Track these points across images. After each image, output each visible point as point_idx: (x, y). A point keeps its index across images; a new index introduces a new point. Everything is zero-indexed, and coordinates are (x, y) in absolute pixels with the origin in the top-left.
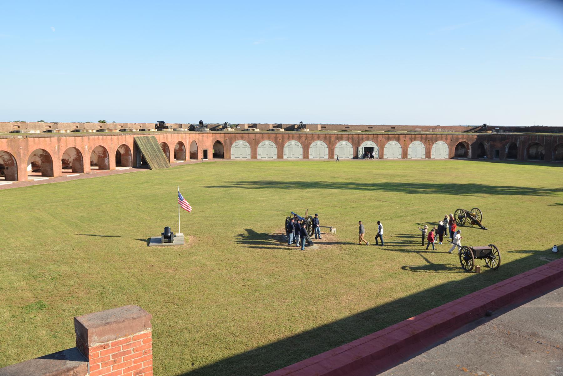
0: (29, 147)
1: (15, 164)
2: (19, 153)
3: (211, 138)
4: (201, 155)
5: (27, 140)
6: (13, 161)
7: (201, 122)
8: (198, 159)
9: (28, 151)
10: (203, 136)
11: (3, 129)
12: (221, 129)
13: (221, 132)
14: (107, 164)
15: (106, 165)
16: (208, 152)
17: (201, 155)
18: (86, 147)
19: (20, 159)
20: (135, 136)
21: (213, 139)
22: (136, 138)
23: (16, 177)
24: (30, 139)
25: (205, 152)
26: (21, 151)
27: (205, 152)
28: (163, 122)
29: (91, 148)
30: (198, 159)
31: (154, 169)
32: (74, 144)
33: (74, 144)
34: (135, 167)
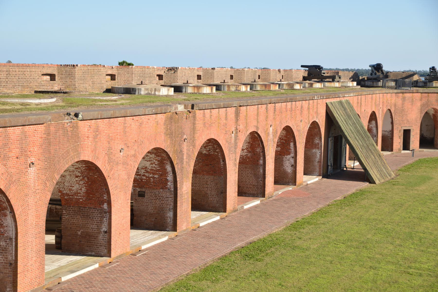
0: (197, 135)
1: (170, 184)
2: (181, 151)
3: (419, 104)
4: (398, 142)
5: (194, 117)
6: (164, 173)
7: (378, 67)
8: (392, 150)
9: (194, 146)
10: (404, 99)
11: (93, 83)
12: (425, 85)
13: (425, 90)
14: (289, 170)
15: (285, 172)
16: (412, 134)
17: (398, 142)
18: (271, 129)
19: (182, 169)
20: (328, 101)
21: (423, 106)
22: (330, 106)
23: (170, 221)
24: (199, 113)
25: (407, 133)
26: (185, 146)
27: (407, 133)
28: (319, 68)
29: (276, 132)
30: (392, 150)
31: (377, 182)
32: (255, 123)
33: (255, 123)
34: (326, 175)
